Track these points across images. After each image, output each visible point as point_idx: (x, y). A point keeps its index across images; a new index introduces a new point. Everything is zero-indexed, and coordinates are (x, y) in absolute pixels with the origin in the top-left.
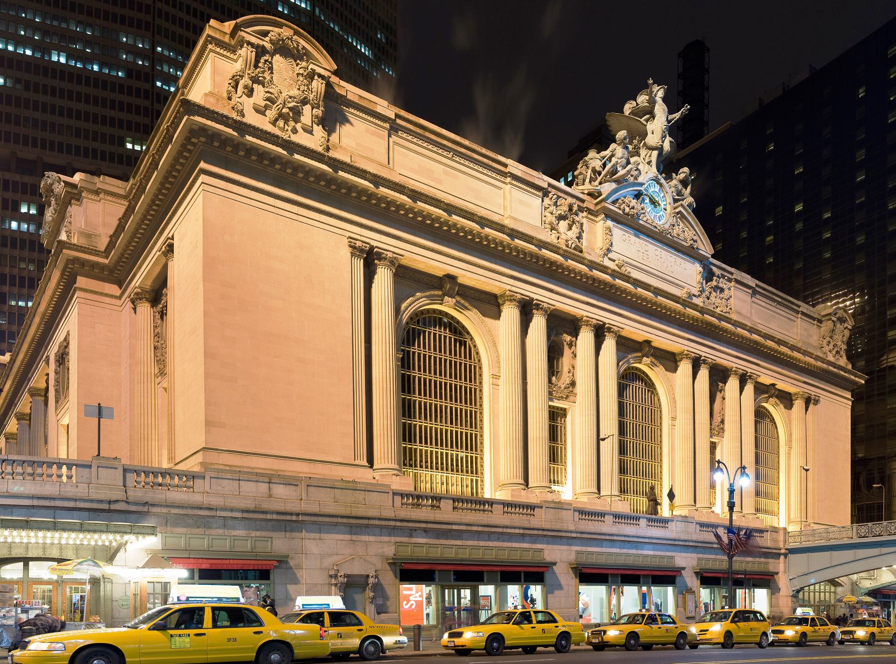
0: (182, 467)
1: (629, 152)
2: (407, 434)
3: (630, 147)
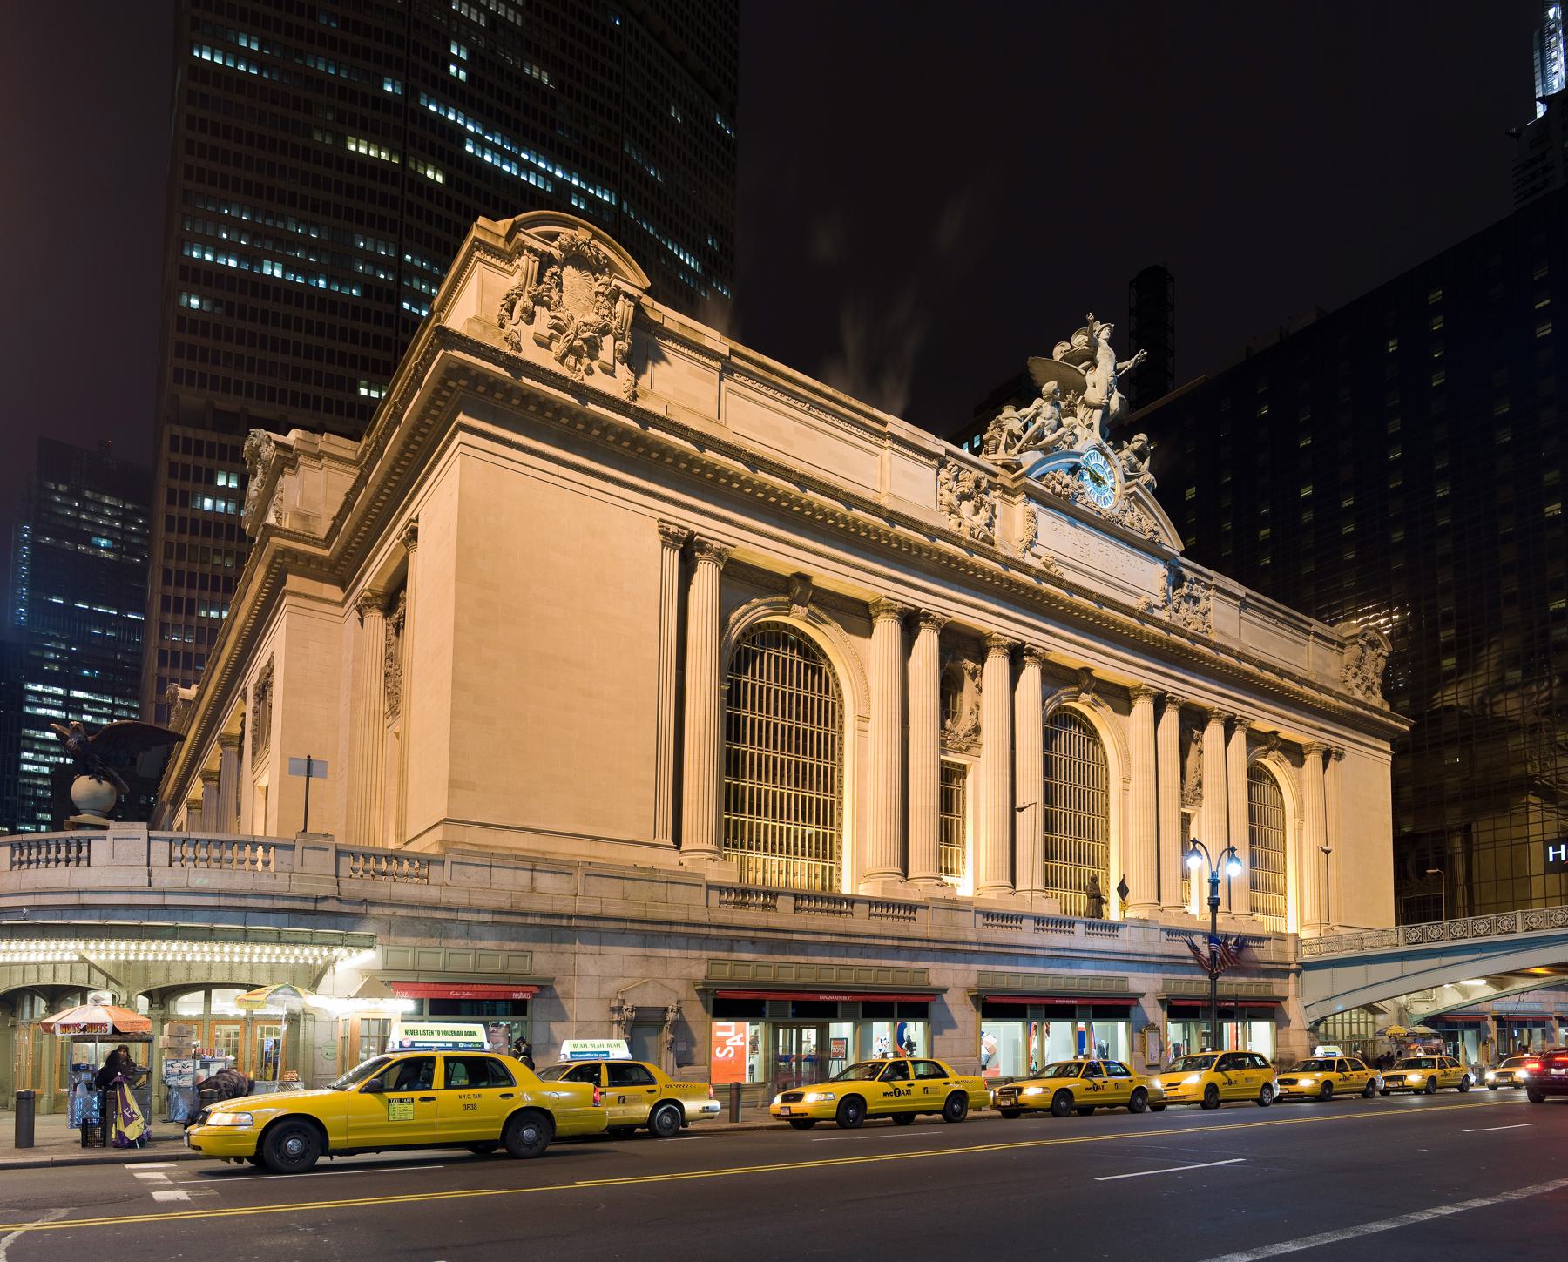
0: (414, 848)
1: (1061, 411)
2: (731, 799)
3: (1063, 404)
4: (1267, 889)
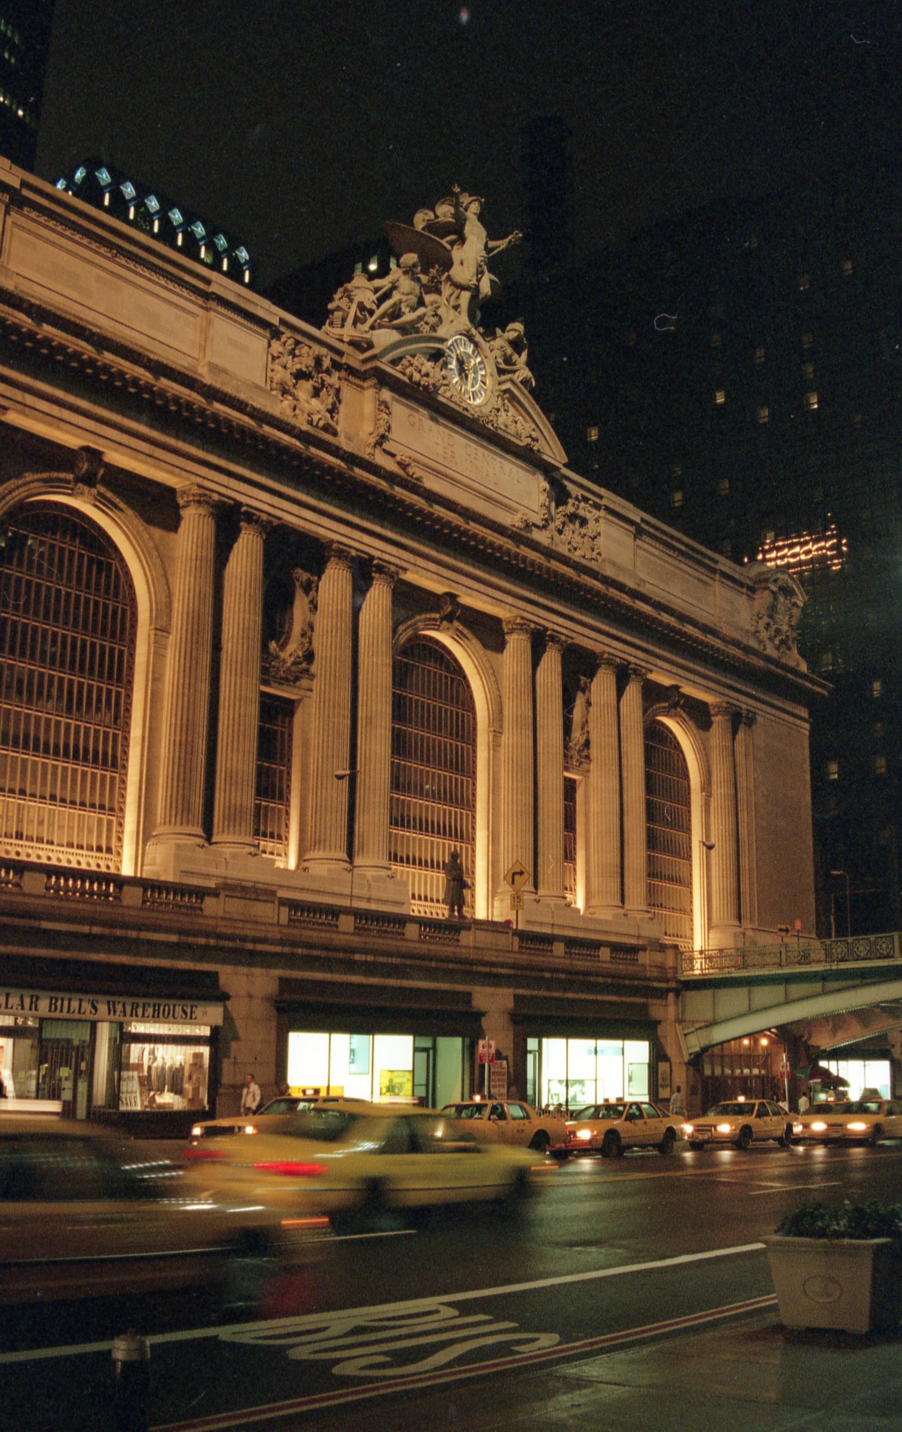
1: (423, 286)
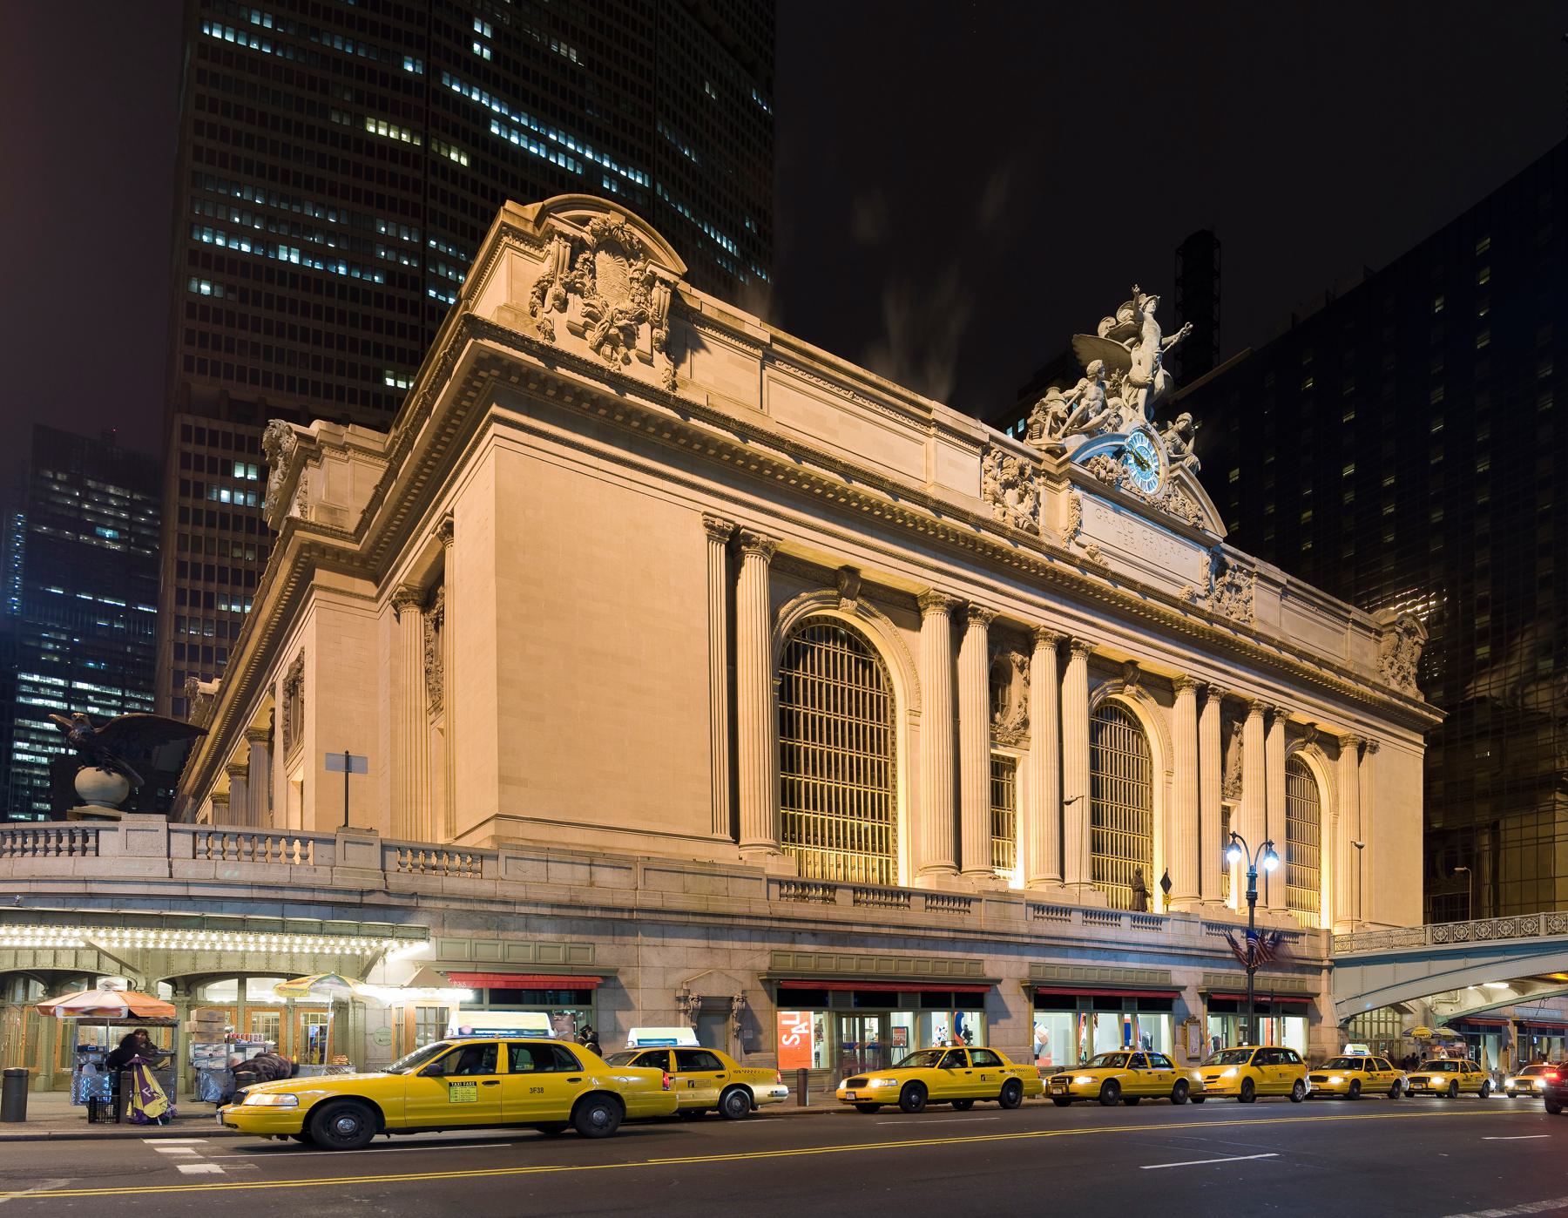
0: (465, 842)
1: (1106, 391)
2: (787, 795)
3: (1108, 384)
4: (1303, 884)
